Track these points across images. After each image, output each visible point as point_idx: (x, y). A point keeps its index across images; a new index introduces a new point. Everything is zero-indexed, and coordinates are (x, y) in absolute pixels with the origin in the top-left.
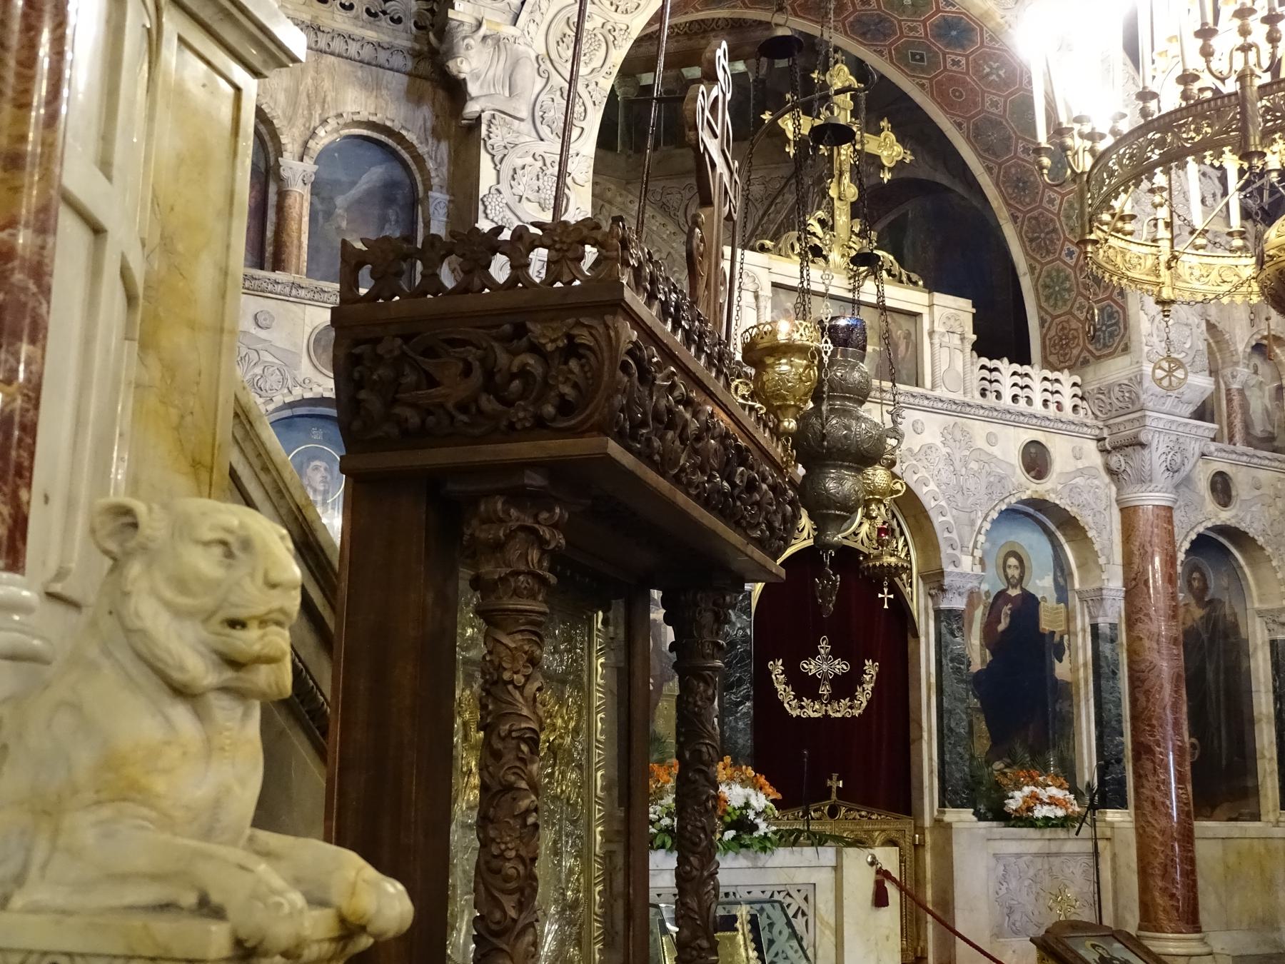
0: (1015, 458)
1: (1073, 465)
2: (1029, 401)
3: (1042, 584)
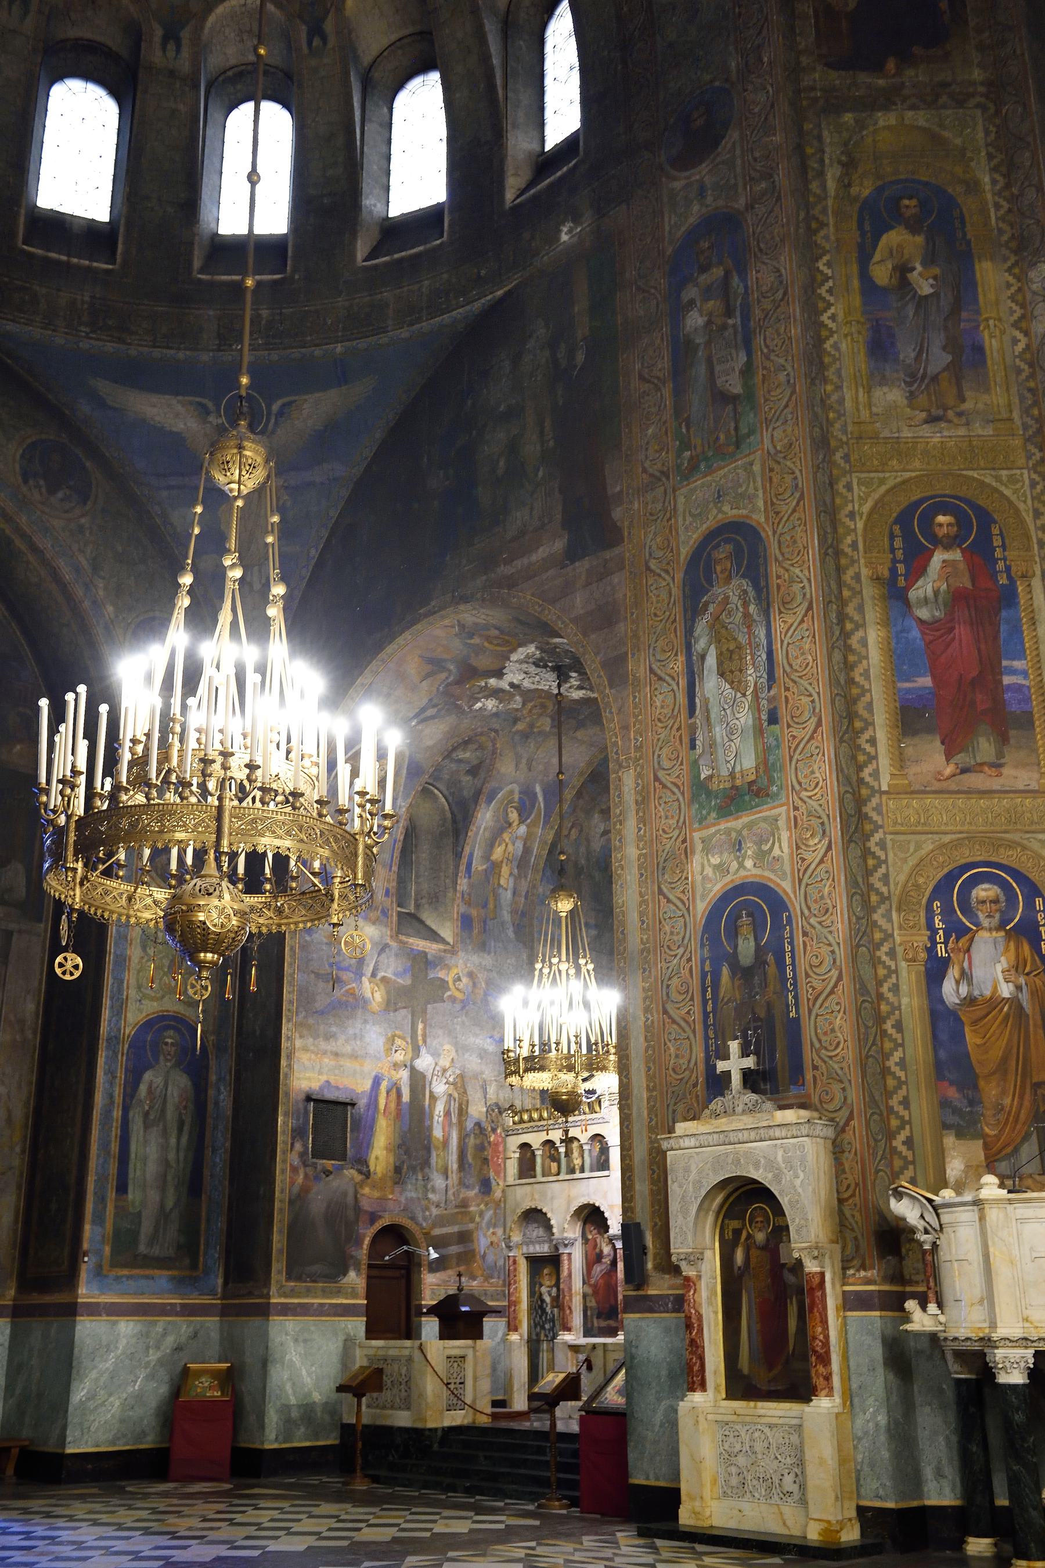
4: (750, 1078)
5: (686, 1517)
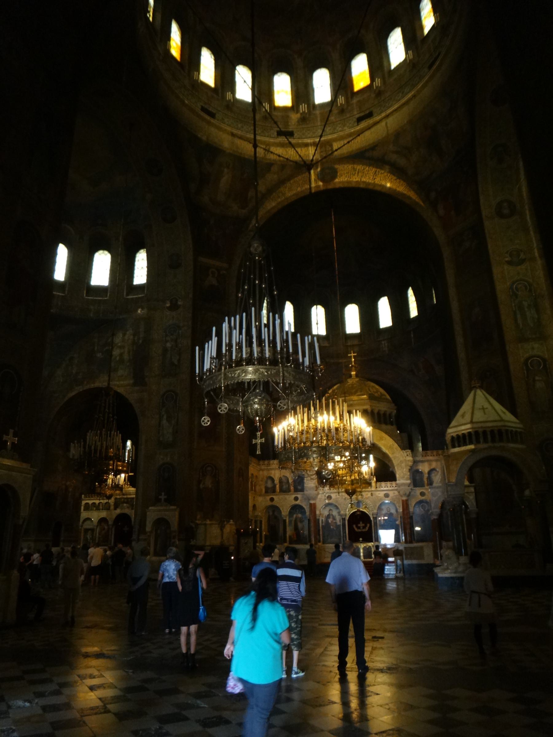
4: (166, 500)
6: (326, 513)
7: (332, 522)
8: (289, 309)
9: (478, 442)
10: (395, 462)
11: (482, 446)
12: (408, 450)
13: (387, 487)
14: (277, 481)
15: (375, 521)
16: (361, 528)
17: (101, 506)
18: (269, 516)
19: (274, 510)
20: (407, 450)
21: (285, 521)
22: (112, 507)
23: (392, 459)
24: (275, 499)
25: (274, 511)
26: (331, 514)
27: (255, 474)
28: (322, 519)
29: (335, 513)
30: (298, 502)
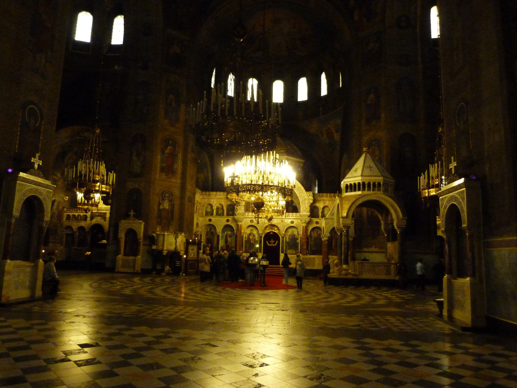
0: (290, 222)
1: (297, 222)
2: (293, 216)
3: (296, 233)
4: (134, 216)
5: (116, 270)
6: (248, 231)
7: (252, 238)
8: (231, 80)
9: (364, 189)
10: (301, 200)
11: (366, 192)
12: (311, 192)
13: (293, 216)
14: (215, 208)
15: (283, 239)
16: (272, 243)
17: (79, 217)
18: (207, 232)
19: (211, 228)
20: (309, 192)
21: (218, 236)
22: (89, 219)
23: (299, 197)
24: (212, 220)
25: (211, 229)
26: (252, 233)
27: (199, 201)
28: (245, 236)
29: (255, 232)
30: (229, 223)
